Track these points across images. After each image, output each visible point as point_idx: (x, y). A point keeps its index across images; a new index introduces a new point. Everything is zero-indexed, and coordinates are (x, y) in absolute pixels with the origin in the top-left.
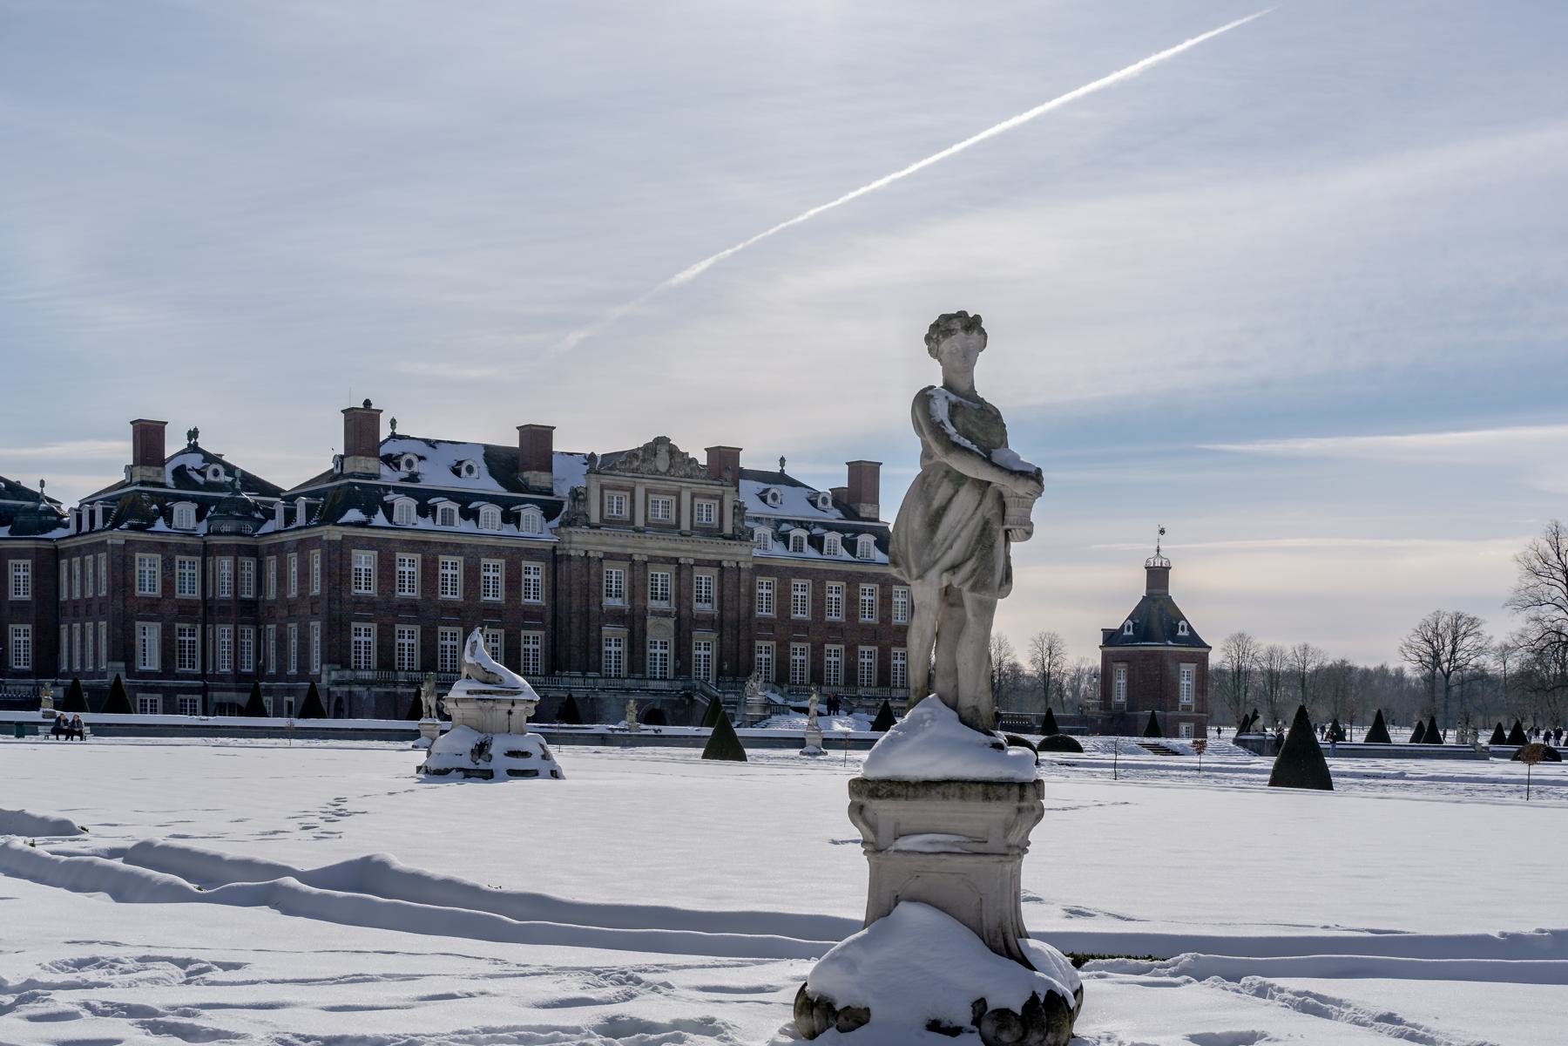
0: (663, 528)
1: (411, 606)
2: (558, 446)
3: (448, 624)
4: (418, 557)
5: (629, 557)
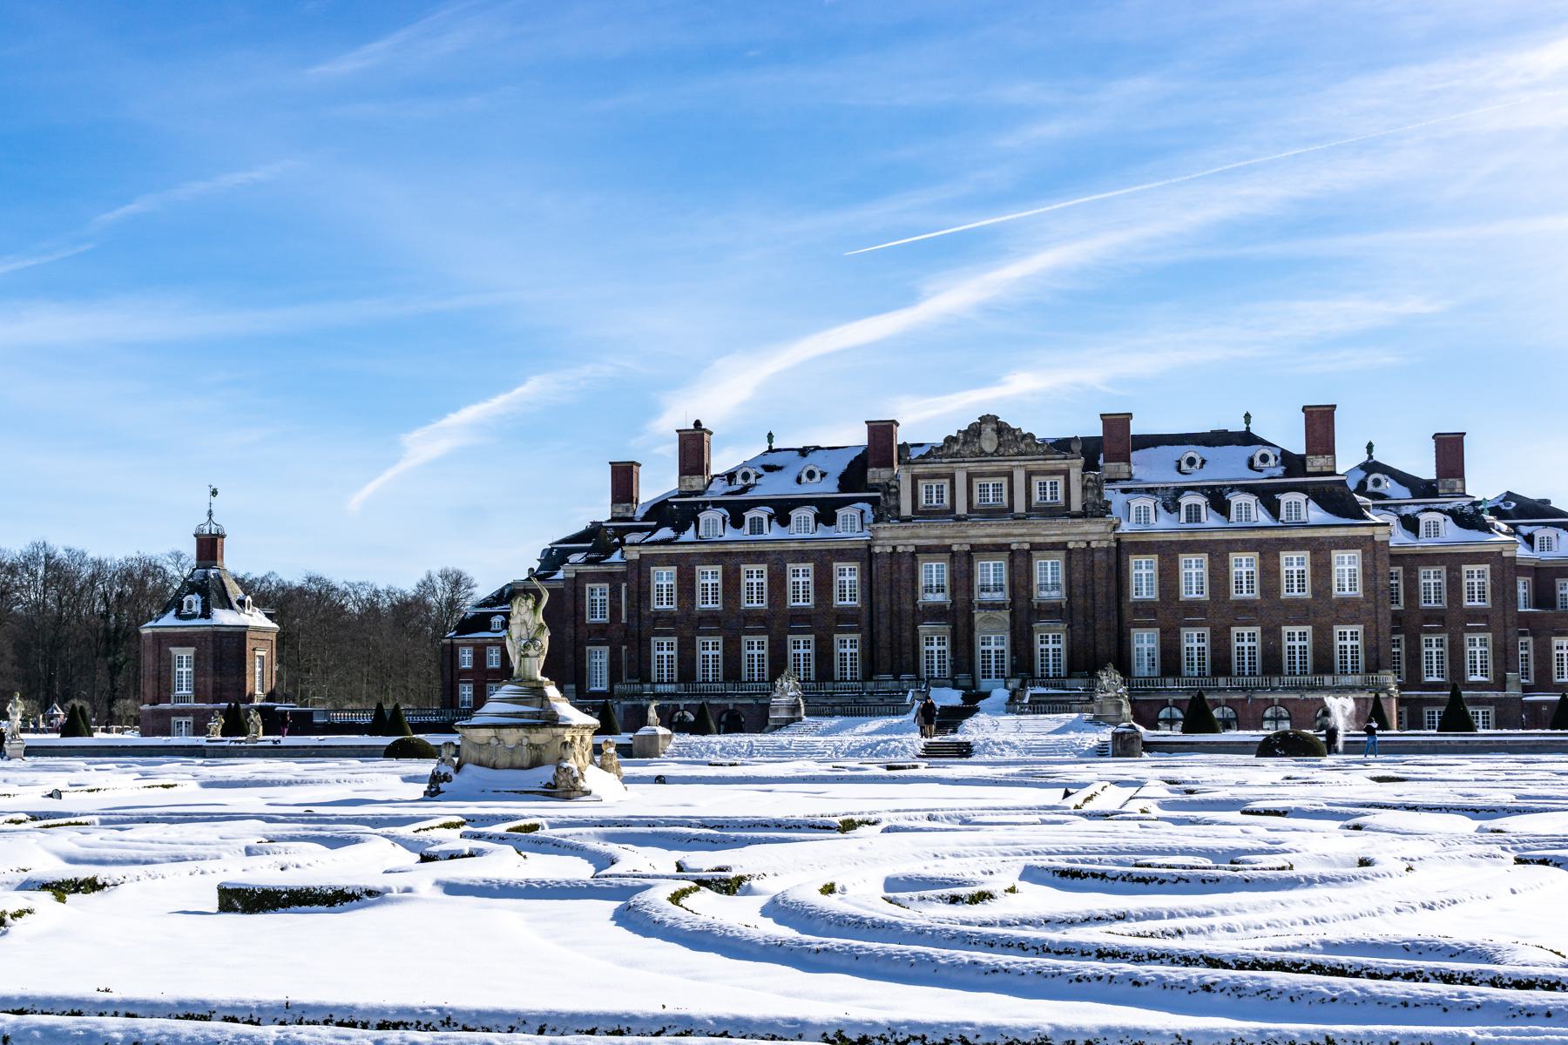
0: (991, 514)
1: (711, 617)
2: (901, 437)
3: (752, 633)
4: (719, 569)
5: (947, 549)
